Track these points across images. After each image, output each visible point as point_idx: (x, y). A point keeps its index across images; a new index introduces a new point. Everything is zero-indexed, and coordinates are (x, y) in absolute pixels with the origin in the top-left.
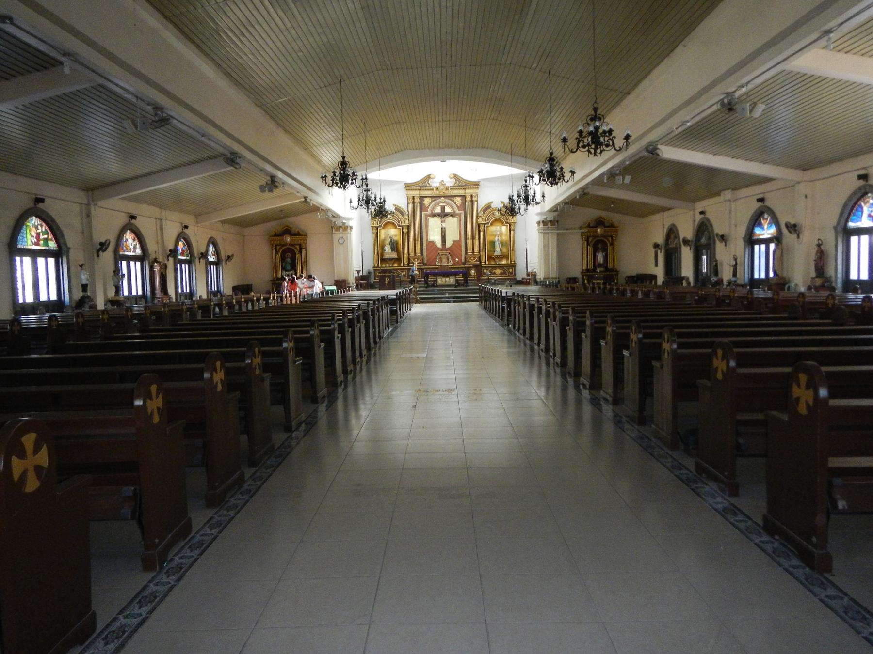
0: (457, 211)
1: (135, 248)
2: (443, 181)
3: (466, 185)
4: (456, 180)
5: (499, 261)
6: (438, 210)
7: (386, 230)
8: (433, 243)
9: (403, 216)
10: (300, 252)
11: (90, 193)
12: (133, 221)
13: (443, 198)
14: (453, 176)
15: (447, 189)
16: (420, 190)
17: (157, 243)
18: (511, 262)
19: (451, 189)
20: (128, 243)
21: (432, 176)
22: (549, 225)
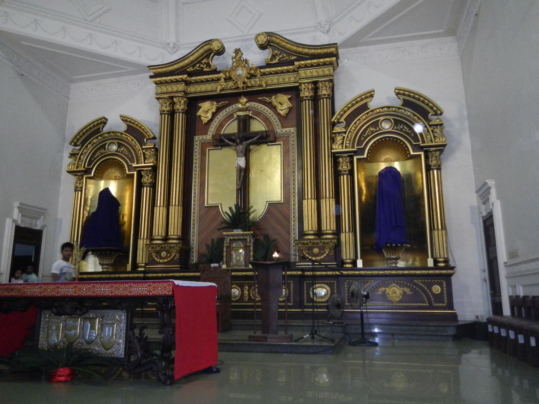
0: (279, 130)
3: (299, 59)
4: (274, 48)
5: (398, 259)
6: (232, 128)
9: (141, 143)
13: (244, 100)
14: (263, 39)
15: (252, 76)
16: (188, 83)
18: (436, 262)
19: (264, 74)
21: (215, 46)
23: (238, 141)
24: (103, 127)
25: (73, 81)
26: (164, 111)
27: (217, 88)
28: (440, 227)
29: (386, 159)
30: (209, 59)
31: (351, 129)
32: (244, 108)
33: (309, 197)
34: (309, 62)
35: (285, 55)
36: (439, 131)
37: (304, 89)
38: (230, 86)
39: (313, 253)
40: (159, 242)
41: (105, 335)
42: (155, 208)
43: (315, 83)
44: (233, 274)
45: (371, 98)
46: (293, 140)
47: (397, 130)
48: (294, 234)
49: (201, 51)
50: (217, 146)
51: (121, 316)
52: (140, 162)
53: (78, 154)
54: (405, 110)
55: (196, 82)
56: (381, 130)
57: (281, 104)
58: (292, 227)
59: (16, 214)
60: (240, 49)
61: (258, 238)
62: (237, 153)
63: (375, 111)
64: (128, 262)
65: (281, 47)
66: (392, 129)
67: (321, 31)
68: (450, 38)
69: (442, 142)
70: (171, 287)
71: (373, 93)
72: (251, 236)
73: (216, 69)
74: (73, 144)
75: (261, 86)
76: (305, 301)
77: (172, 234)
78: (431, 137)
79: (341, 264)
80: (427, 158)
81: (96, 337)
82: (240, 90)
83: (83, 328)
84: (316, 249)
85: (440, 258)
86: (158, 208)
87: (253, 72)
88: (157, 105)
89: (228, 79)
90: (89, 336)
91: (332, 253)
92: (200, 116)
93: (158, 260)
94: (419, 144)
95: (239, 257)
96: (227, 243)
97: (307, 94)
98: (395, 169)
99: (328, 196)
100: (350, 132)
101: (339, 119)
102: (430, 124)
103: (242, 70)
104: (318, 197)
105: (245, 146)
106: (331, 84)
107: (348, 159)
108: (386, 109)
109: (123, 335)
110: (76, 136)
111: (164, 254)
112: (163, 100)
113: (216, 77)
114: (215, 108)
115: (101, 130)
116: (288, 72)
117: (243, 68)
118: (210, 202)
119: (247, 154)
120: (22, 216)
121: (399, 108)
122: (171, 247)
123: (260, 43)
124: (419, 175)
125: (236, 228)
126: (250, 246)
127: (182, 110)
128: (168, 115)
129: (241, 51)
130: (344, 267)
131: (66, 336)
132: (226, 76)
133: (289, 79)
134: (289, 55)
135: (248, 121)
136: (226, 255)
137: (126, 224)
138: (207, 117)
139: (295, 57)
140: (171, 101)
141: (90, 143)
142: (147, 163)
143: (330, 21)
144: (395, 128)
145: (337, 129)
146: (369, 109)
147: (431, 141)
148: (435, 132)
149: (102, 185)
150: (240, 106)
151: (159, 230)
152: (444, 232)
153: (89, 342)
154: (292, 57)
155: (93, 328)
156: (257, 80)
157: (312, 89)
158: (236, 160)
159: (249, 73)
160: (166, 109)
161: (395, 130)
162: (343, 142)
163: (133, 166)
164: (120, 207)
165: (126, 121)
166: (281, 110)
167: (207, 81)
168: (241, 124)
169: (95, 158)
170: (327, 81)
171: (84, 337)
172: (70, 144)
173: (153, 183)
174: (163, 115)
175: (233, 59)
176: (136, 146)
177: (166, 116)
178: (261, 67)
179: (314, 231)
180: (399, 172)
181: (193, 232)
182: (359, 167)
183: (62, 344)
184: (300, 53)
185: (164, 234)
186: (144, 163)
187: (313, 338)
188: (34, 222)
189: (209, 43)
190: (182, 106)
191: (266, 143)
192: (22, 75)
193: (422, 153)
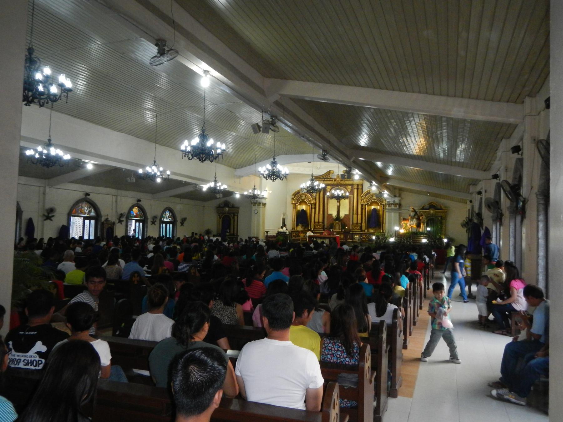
1: (90, 212)
7: (301, 206)
8: (331, 215)
10: (234, 218)
11: (47, 180)
12: (88, 197)
17: (112, 209)
20: (83, 209)
21: (332, 172)
22: (393, 206)
48: (351, 223)
79: (362, 231)
80: (383, 206)
89: (335, 180)
119: (339, 202)
145: (363, 198)
151: (317, 220)
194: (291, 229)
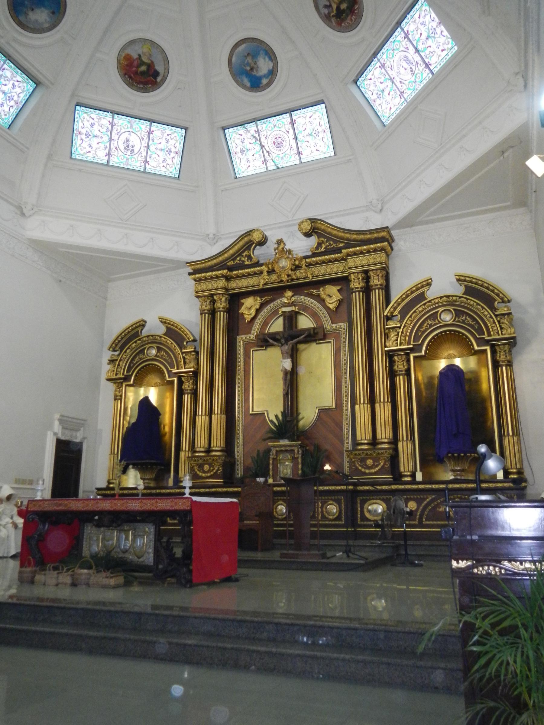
0: (328, 325)
2: (280, 242)
4: (319, 235)
13: (289, 293)
14: (307, 227)
15: (297, 267)
16: (228, 279)
19: (309, 265)
21: (256, 237)
23: (283, 341)
24: (142, 330)
25: (109, 281)
26: (204, 310)
27: (259, 282)
28: (511, 433)
29: (449, 354)
30: (250, 250)
31: (406, 323)
32: (289, 303)
33: (362, 402)
34: (358, 248)
35: (332, 243)
36: (507, 321)
37: (354, 279)
38: (273, 279)
39: (366, 465)
40: (201, 454)
41: (137, 545)
42: (197, 417)
43: (366, 272)
44: (275, 489)
45: (429, 286)
46: (344, 337)
47: (459, 321)
48: (348, 445)
49: (241, 243)
50: (262, 346)
51: (150, 529)
52: (180, 367)
53: (117, 360)
54: (467, 299)
55: (238, 277)
56: (440, 323)
57: (330, 296)
58: (345, 436)
59: (57, 427)
60: (282, 239)
61: (308, 448)
62: (282, 353)
63: (433, 301)
64: (170, 477)
65: (327, 234)
66: (453, 321)
67: (373, 210)
68: (522, 210)
69: (511, 334)
70: (190, 502)
71: (430, 281)
72: (299, 447)
73: (258, 261)
74: (111, 349)
75: (306, 277)
76: (359, 520)
77: (215, 445)
78: (497, 328)
79: (397, 477)
80: (494, 352)
81: (130, 547)
82: (284, 283)
83: (118, 540)
84: (369, 460)
85: (512, 468)
86: (200, 417)
87: (297, 263)
88: (197, 303)
89: (271, 272)
90: (124, 546)
91: (387, 465)
92: (243, 314)
93: (200, 474)
94: (484, 338)
95: (286, 470)
96: (273, 455)
97: (357, 285)
98: (458, 367)
99: (382, 400)
100: (405, 326)
101: (392, 313)
102: (496, 313)
103: (286, 262)
104: (372, 402)
105: (291, 345)
106: (384, 272)
107: (404, 356)
108: (445, 298)
109: (152, 544)
110: (115, 341)
111: (206, 467)
112: (203, 298)
113: (258, 271)
114: (259, 304)
115: (140, 333)
116: (336, 260)
117: (287, 259)
118: (255, 410)
119: (294, 355)
120: (63, 428)
121: (460, 297)
122: (213, 460)
123: (304, 232)
124: (484, 374)
125: (283, 439)
126: (298, 458)
127: (223, 308)
128: (209, 314)
129: (283, 242)
130: (402, 481)
131: (104, 546)
132: (269, 268)
133: (338, 268)
134: (335, 242)
135: (294, 319)
136: (273, 468)
137: (168, 434)
138: (250, 315)
139: (343, 244)
140: (212, 299)
141: (128, 348)
142: (187, 368)
143: (381, 200)
144: (457, 320)
145: (391, 324)
146: (426, 299)
147: (498, 333)
148: (503, 323)
149: (142, 392)
150: (285, 300)
151: (201, 442)
152: (515, 438)
153: (125, 551)
154: (339, 244)
155: (127, 538)
156: (302, 271)
157: (363, 279)
158: (282, 362)
159: (294, 265)
160: (206, 308)
161: (458, 321)
162: (398, 338)
163: (173, 371)
164: (160, 417)
165: (165, 323)
166: (330, 303)
167: (249, 275)
168: (286, 321)
169: (134, 365)
170: (379, 269)
171: (119, 547)
172: (109, 350)
173: (194, 390)
174: (203, 315)
175: (275, 250)
176: (175, 350)
177: (207, 315)
178: (306, 257)
179: (367, 440)
180: (462, 370)
181: (238, 443)
182: (416, 367)
183: (102, 553)
184: (348, 239)
185: (206, 446)
186: (185, 368)
187: (348, 556)
188: (74, 434)
189: (249, 234)
190: (223, 304)
191: (315, 341)
192: (60, 281)
193: (488, 348)
194: (104, 485)
